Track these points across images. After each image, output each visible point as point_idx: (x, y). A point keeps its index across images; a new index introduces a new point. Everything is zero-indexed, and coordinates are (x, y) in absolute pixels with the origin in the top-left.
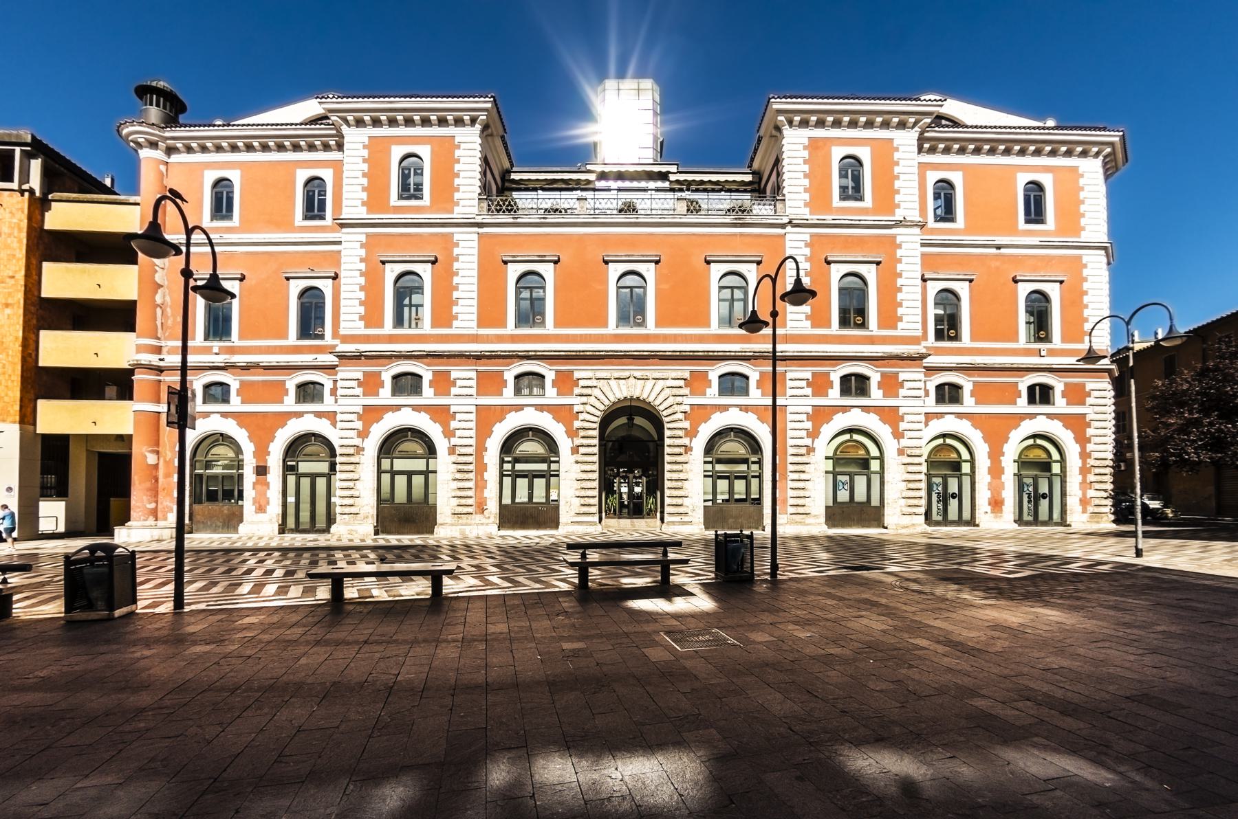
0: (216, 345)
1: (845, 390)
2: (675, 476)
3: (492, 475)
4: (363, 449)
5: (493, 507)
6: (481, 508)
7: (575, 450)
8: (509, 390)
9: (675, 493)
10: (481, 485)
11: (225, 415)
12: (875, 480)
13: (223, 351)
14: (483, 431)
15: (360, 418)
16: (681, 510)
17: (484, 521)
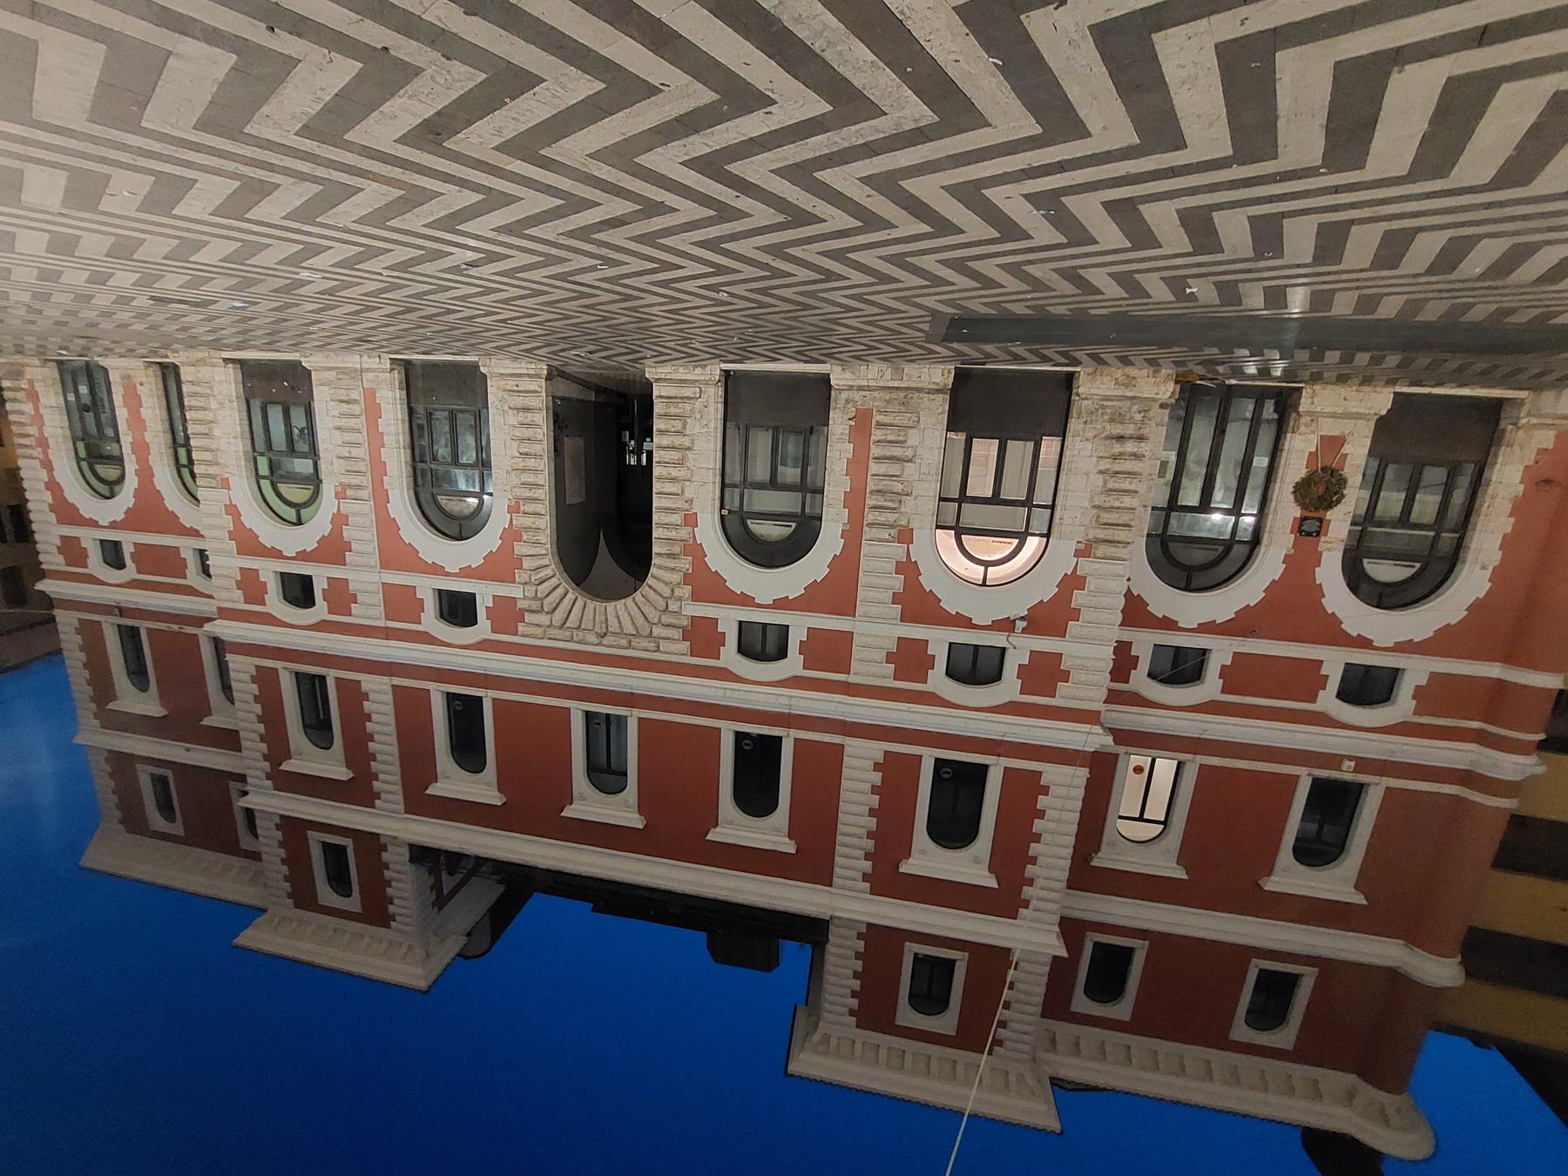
0: (1346, 773)
1: (306, 582)
2: (531, 463)
3: (836, 486)
4: (1078, 554)
5: (839, 424)
6: (862, 423)
7: (691, 520)
8: (796, 638)
9: (528, 433)
10: (858, 466)
11: (1364, 643)
12: (261, 446)
13: (1334, 761)
14: (846, 569)
15: (1075, 614)
16: (519, 401)
17: (858, 396)
